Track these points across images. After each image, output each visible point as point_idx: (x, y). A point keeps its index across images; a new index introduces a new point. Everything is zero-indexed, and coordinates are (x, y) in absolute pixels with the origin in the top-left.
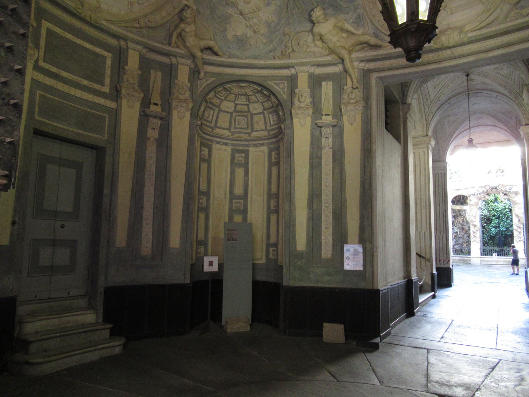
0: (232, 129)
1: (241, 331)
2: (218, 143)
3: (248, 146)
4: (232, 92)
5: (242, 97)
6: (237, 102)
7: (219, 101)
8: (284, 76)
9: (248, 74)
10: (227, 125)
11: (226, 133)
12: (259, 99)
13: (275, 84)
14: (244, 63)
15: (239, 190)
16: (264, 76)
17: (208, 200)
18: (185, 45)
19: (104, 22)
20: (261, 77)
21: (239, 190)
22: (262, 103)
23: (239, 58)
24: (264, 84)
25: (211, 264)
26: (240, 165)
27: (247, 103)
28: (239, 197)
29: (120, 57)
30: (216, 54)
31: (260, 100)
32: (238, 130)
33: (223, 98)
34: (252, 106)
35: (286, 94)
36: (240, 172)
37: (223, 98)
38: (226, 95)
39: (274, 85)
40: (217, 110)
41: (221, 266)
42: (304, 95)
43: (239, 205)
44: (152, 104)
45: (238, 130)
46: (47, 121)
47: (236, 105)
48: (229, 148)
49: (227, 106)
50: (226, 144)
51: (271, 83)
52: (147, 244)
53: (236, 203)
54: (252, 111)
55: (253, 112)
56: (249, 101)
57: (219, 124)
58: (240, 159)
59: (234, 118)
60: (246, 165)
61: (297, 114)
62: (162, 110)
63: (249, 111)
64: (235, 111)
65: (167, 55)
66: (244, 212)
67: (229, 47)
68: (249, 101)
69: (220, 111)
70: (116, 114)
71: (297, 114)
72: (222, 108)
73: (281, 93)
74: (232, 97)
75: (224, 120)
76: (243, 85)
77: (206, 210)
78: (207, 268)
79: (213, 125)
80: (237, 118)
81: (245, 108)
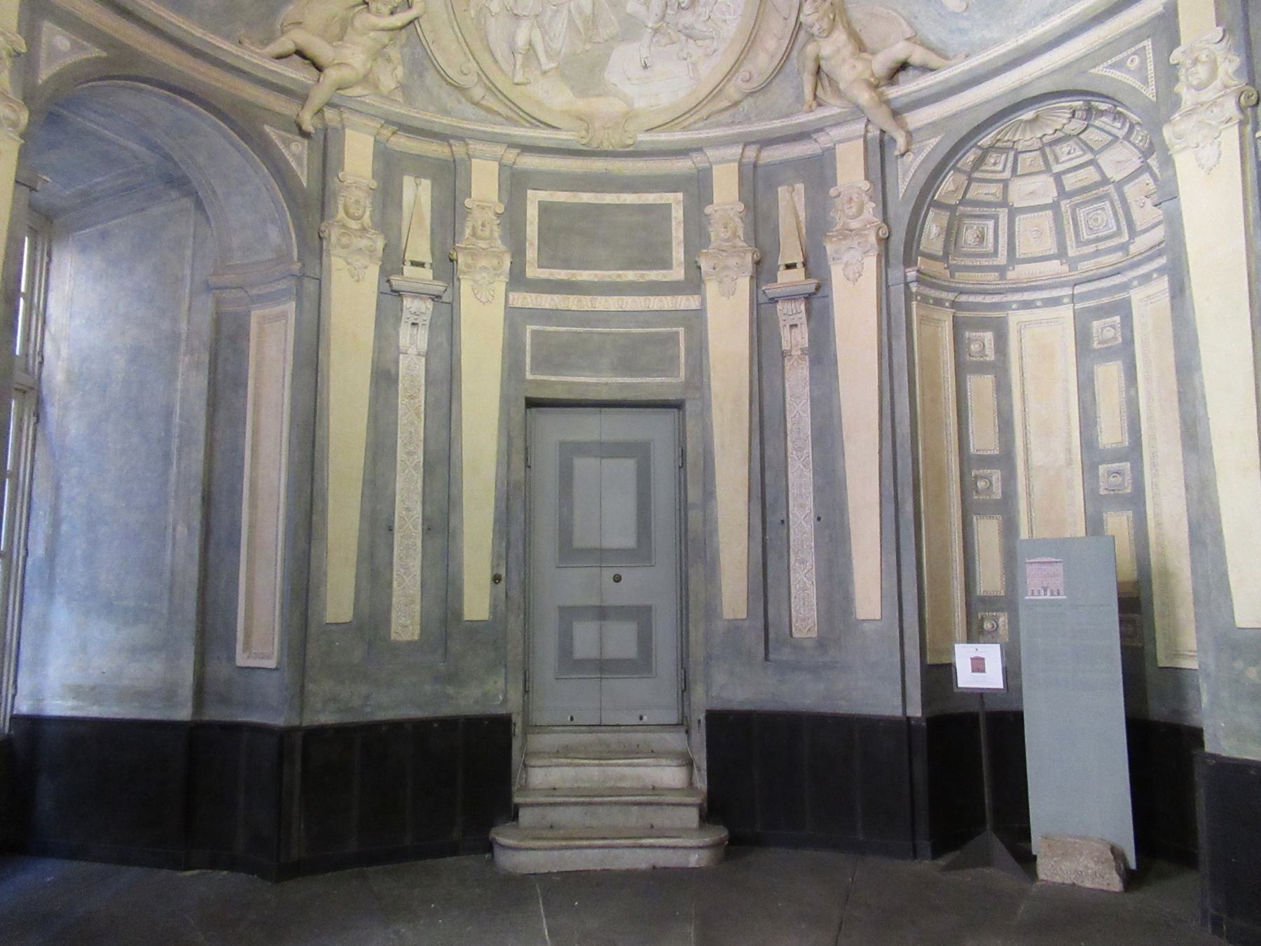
0: (1072, 252)
1: (1088, 884)
2: (1027, 305)
3: (1125, 287)
4: (1020, 147)
5: (1065, 148)
6: (1057, 168)
7: (995, 189)
8: (1139, 28)
9: (1027, 79)
10: (1048, 244)
11: (1054, 267)
12: (1115, 131)
13: (1112, 66)
14: (1004, 55)
15: (1111, 434)
16: (1079, 60)
17: (1009, 479)
18: (838, 93)
19: (643, 137)
20: (1068, 66)
21: (1111, 434)
22: (1127, 137)
23: (996, 42)
24: (1081, 84)
25: (978, 665)
26: (1108, 354)
27: (1089, 157)
28: (1117, 455)
29: (698, 188)
30: (926, 69)
31: (1121, 134)
32: (1091, 249)
33: (1007, 174)
34: (1105, 160)
35: (1152, 81)
36: (1109, 375)
37: (1007, 174)
38: (1009, 165)
39: (1116, 74)
40: (1003, 214)
41: (1011, 671)
42: (1203, 58)
43: (1119, 479)
44: (782, 268)
45: (1091, 249)
46: (553, 378)
47: (1058, 178)
48: (1065, 313)
49: (1033, 189)
50: (1056, 302)
51: (1099, 70)
52: (406, 622)
53: (1110, 473)
54: (1114, 174)
55: (1117, 178)
56: (1091, 149)
57: (1019, 253)
58: (1109, 333)
59: (1067, 218)
60: (1125, 351)
61: (1179, 137)
62: (808, 275)
63: (1105, 181)
64: (1063, 193)
65: (802, 135)
66: (1136, 500)
67: (961, 31)
68: (1091, 149)
69: (1013, 213)
70: (695, 321)
71: (1179, 137)
72: (1016, 200)
73: (1137, 85)
74: (1026, 160)
75: (1035, 235)
76: (1028, 115)
77: (1006, 509)
78: (966, 679)
79: (1002, 259)
80: (1081, 213)
81: (1090, 175)
